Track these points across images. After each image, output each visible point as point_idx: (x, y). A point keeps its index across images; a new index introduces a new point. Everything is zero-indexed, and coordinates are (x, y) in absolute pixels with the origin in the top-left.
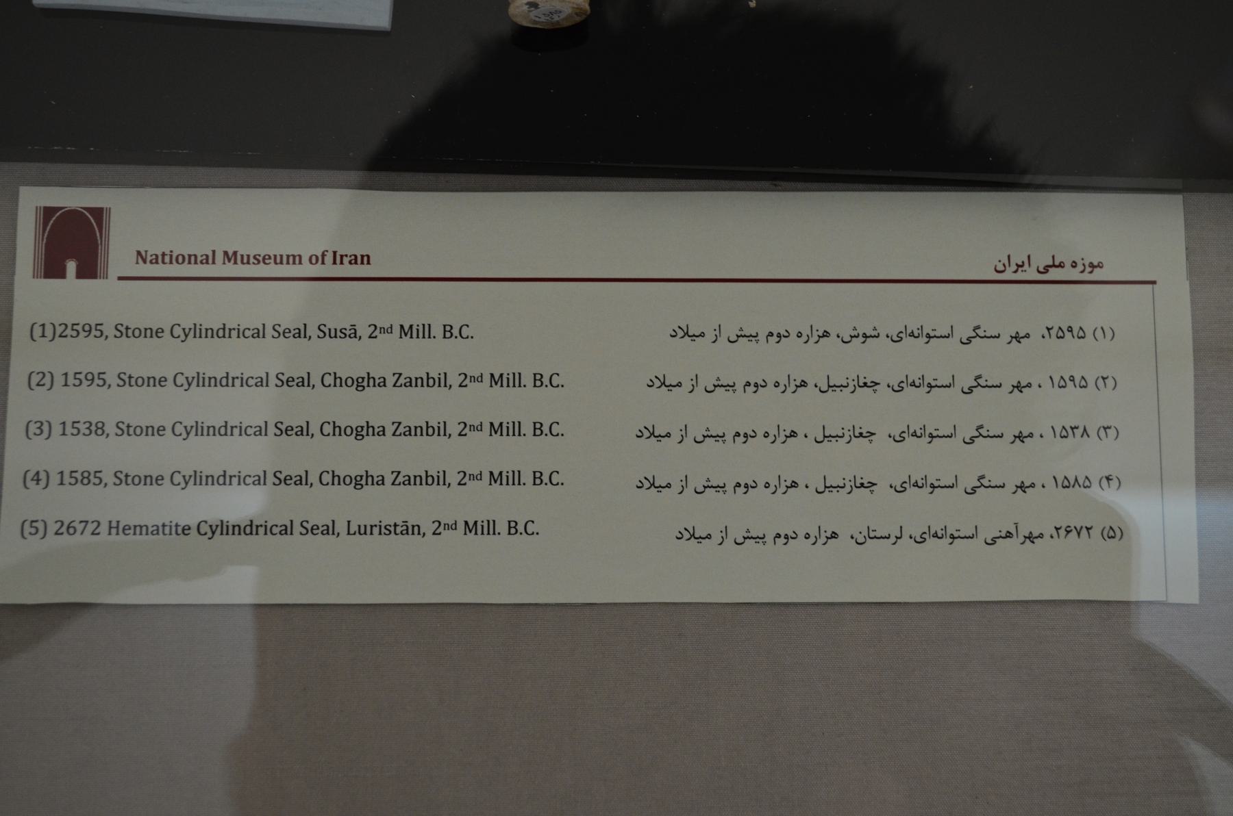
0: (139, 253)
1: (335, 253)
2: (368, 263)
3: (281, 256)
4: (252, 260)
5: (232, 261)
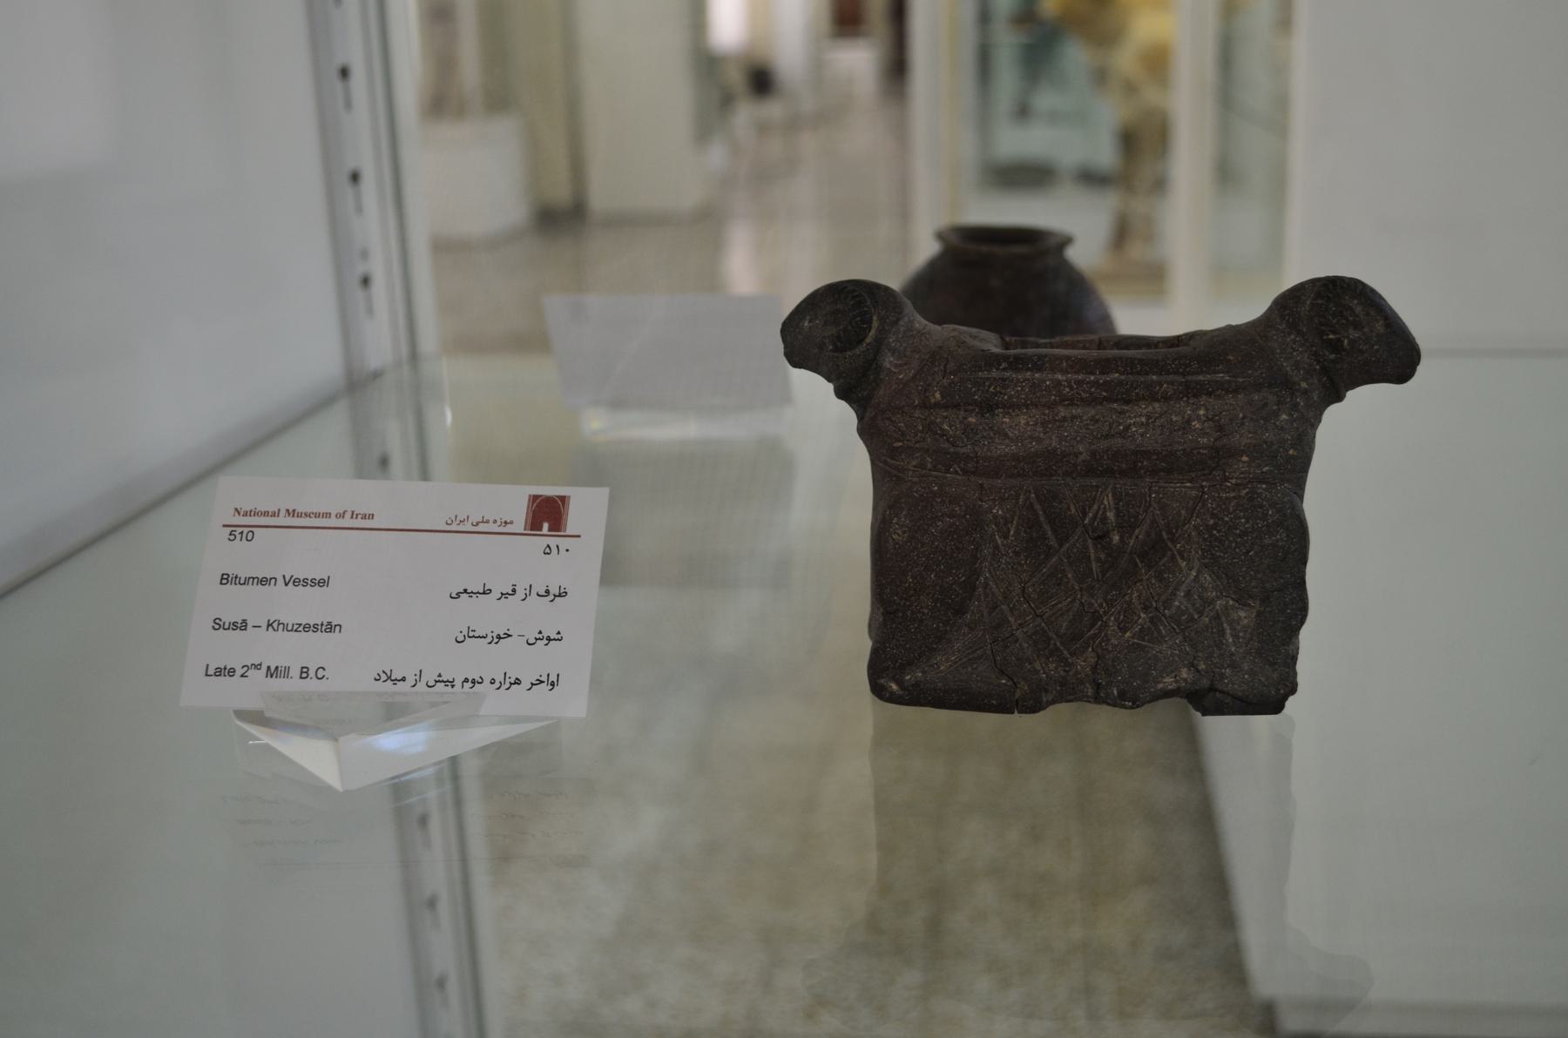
0: (236, 509)
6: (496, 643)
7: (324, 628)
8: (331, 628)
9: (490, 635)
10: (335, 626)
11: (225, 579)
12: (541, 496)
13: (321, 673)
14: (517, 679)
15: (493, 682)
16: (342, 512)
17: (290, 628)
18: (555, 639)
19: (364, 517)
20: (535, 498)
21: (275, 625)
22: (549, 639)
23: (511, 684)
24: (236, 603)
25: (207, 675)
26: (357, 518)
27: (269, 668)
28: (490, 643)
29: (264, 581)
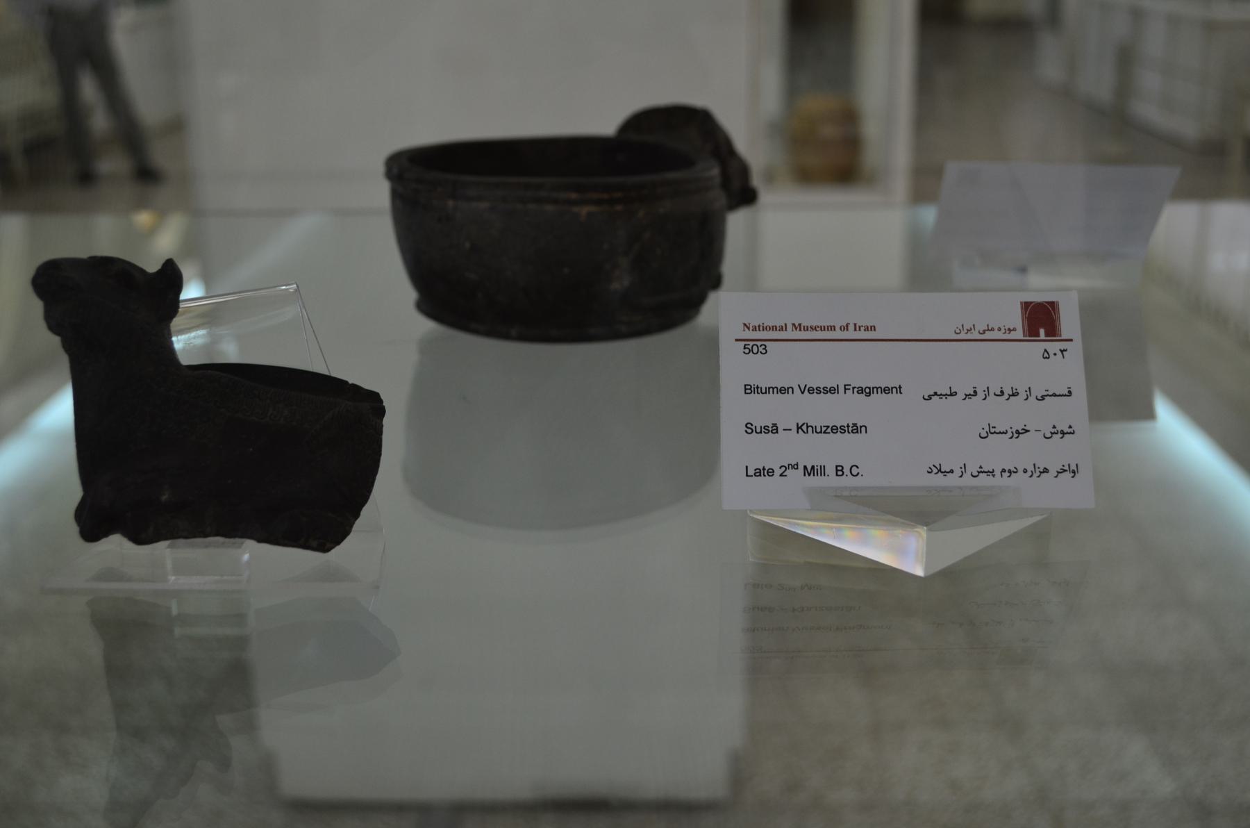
0: (745, 325)
1: (855, 325)
2: (875, 330)
3: (824, 327)
4: (809, 329)
5: (798, 329)
6: (1017, 438)
7: (850, 429)
9: (1010, 431)
10: (861, 427)
11: (749, 389)
12: (1031, 303)
13: (855, 471)
14: (1045, 468)
15: (1025, 471)
16: (845, 325)
17: (818, 430)
18: (1067, 433)
19: (867, 329)
20: (1026, 305)
21: (804, 428)
22: (1063, 433)
23: (1041, 472)
24: (764, 409)
25: (747, 475)
26: (860, 330)
27: (805, 467)
28: (1011, 438)
29: (783, 390)
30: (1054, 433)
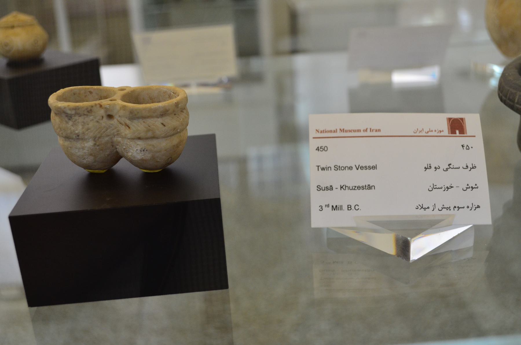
6: (447, 190)
7: (367, 187)
8: (370, 187)
17: (351, 188)
18: (474, 188)
21: (344, 187)
22: (472, 188)
30: (468, 188)
